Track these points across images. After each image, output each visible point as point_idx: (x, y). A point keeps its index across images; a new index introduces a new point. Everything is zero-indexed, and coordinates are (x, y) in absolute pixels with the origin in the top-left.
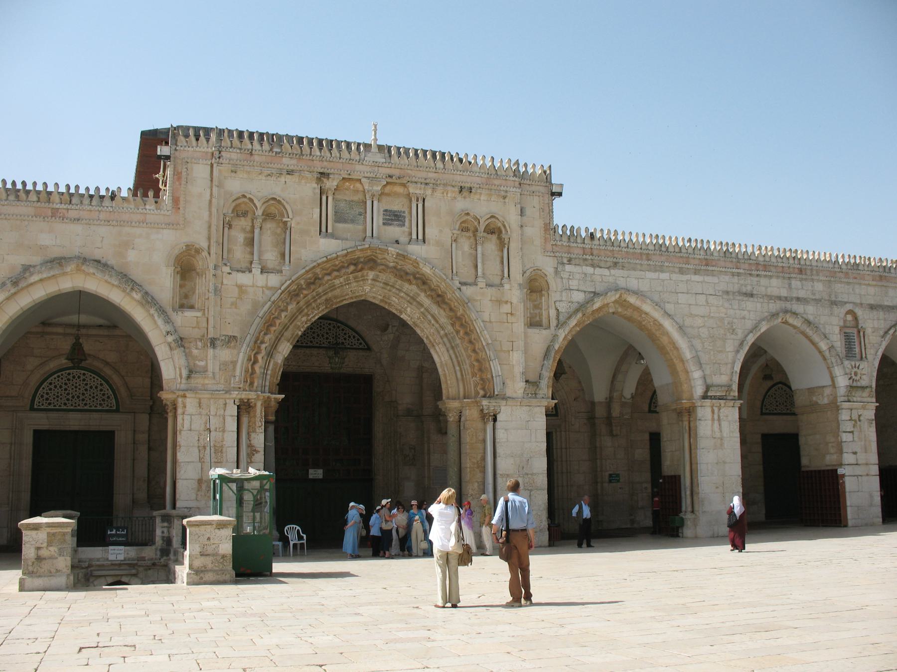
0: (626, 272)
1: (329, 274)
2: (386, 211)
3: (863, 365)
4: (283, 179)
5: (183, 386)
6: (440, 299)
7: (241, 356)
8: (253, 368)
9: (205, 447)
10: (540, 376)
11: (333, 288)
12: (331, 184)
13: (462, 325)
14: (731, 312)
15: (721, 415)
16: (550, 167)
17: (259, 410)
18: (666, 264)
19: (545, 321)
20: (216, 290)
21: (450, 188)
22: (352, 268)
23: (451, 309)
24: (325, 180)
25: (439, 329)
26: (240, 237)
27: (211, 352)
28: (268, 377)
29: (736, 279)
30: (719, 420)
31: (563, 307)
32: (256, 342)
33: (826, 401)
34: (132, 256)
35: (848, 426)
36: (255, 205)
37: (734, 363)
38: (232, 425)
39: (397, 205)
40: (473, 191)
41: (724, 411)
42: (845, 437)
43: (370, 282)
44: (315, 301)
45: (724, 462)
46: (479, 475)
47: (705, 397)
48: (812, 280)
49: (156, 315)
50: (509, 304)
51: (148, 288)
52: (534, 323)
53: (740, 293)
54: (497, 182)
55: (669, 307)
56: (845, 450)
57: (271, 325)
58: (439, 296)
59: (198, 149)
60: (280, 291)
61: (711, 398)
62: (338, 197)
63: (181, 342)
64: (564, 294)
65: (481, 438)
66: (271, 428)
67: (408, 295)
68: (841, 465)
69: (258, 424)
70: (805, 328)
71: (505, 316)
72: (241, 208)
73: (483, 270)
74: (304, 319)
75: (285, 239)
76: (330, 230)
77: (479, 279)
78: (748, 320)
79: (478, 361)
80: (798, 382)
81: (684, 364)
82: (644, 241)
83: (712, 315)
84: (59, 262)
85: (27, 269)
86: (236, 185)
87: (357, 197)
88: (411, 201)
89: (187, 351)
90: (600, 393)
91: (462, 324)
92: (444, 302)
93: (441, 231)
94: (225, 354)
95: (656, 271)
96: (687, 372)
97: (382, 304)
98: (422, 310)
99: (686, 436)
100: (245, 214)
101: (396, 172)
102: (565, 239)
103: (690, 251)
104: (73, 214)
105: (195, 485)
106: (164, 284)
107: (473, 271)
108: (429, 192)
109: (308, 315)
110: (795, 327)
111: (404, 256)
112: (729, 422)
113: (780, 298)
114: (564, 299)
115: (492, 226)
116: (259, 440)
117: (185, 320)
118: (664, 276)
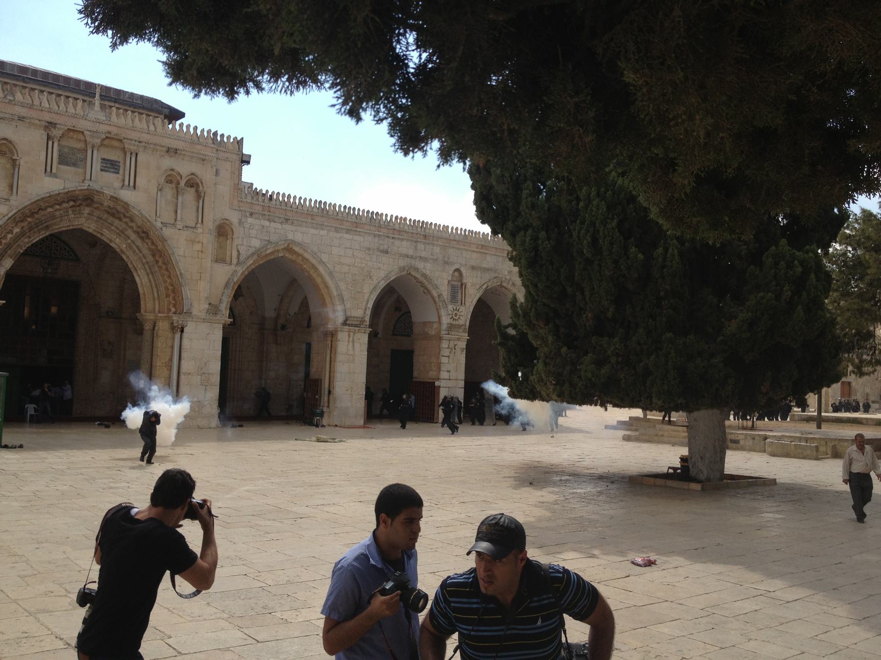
3: (462, 308)
6: (144, 234)
10: (221, 301)
11: (53, 217)
19: (228, 259)
21: (158, 147)
22: (72, 203)
23: (153, 243)
24: (52, 129)
33: (433, 333)
35: (445, 352)
37: (368, 301)
39: (114, 155)
41: (358, 335)
42: (444, 360)
45: (354, 373)
47: (345, 323)
48: (433, 244)
52: (220, 260)
53: (379, 250)
54: (199, 147)
55: (325, 258)
56: (442, 369)
58: (144, 232)
60: (7, 218)
61: (349, 325)
62: (62, 143)
64: (245, 240)
68: (438, 379)
70: (422, 279)
74: (26, 240)
76: (54, 171)
77: (178, 223)
78: (383, 271)
79: (172, 285)
80: (417, 318)
87: (80, 145)
88: (125, 153)
90: (270, 313)
92: (148, 237)
99: (329, 352)
101: (114, 130)
102: (249, 197)
108: (141, 149)
110: (416, 278)
111: (116, 198)
113: (407, 256)
115: (192, 182)
118: (323, 233)
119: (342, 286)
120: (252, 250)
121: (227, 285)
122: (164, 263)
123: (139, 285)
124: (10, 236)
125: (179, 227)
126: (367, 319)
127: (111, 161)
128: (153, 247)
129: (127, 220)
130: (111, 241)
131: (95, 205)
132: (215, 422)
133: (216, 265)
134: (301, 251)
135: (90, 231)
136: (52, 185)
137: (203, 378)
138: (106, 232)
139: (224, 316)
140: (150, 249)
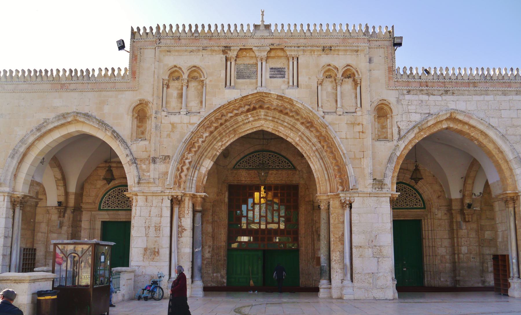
0: (455, 97)
1: (231, 112)
2: (272, 69)
4: (201, 53)
6: (310, 124)
7: (171, 168)
8: (180, 176)
10: (385, 176)
12: (232, 54)
16: (393, 27)
17: (188, 204)
18: (491, 89)
19: (389, 136)
20: (156, 127)
21: (315, 48)
23: (317, 131)
24: (229, 52)
25: (312, 146)
26: (173, 92)
27: (152, 166)
28: (194, 182)
31: (404, 127)
32: (182, 159)
34: (106, 109)
36: (182, 71)
38: (167, 213)
39: (278, 64)
40: (332, 48)
43: (263, 117)
44: (225, 131)
46: (340, 246)
49: (120, 145)
50: (361, 126)
52: (382, 136)
54: (350, 41)
55: (494, 122)
57: (192, 147)
58: (309, 122)
60: (196, 125)
62: (239, 61)
63: (134, 161)
64: (404, 116)
65: (342, 220)
66: (198, 215)
67: (289, 124)
69: (186, 212)
71: (358, 134)
72: (175, 74)
73: (342, 103)
74: (220, 144)
75: (202, 93)
76: (232, 84)
79: (338, 166)
81: (508, 163)
82: (471, 74)
84: (64, 116)
85: (46, 122)
86: (171, 61)
87: (252, 61)
88: (288, 59)
89: (139, 166)
91: (326, 141)
92: (312, 126)
93: (310, 78)
94: (161, 167)
95: (482, 94)
96: (511, 169)
97: (273, 132)
98: (300, 133)
100: (178, 78)
101: (276, 42)
104: (72, 87)
105: (142, 251)
106: (126, 125)
107: (335, 104)
108: (301, 53)
109: (223, 141)
114: (404, 119)
115: (349, 73)
116: (187, 222)
117: (139, 148)
118: (487, 98)
120: (413, 124)
121: (390, 160)
122: (328, 147)
123: (314, 171)
124: (201, 140)
125: (339, 113)
127: (279, 68)
128: (318, 134)
129: (294, 114)
130: (287, 137)
131: (266, 106)
132: (391, 292)
133: (378, 143)
134: (466, 119)
135: (270, 130)
136: (232, 95)
137: (375, 250)
138: (281, 129)
139: (391, 189)
140: (318, 137)
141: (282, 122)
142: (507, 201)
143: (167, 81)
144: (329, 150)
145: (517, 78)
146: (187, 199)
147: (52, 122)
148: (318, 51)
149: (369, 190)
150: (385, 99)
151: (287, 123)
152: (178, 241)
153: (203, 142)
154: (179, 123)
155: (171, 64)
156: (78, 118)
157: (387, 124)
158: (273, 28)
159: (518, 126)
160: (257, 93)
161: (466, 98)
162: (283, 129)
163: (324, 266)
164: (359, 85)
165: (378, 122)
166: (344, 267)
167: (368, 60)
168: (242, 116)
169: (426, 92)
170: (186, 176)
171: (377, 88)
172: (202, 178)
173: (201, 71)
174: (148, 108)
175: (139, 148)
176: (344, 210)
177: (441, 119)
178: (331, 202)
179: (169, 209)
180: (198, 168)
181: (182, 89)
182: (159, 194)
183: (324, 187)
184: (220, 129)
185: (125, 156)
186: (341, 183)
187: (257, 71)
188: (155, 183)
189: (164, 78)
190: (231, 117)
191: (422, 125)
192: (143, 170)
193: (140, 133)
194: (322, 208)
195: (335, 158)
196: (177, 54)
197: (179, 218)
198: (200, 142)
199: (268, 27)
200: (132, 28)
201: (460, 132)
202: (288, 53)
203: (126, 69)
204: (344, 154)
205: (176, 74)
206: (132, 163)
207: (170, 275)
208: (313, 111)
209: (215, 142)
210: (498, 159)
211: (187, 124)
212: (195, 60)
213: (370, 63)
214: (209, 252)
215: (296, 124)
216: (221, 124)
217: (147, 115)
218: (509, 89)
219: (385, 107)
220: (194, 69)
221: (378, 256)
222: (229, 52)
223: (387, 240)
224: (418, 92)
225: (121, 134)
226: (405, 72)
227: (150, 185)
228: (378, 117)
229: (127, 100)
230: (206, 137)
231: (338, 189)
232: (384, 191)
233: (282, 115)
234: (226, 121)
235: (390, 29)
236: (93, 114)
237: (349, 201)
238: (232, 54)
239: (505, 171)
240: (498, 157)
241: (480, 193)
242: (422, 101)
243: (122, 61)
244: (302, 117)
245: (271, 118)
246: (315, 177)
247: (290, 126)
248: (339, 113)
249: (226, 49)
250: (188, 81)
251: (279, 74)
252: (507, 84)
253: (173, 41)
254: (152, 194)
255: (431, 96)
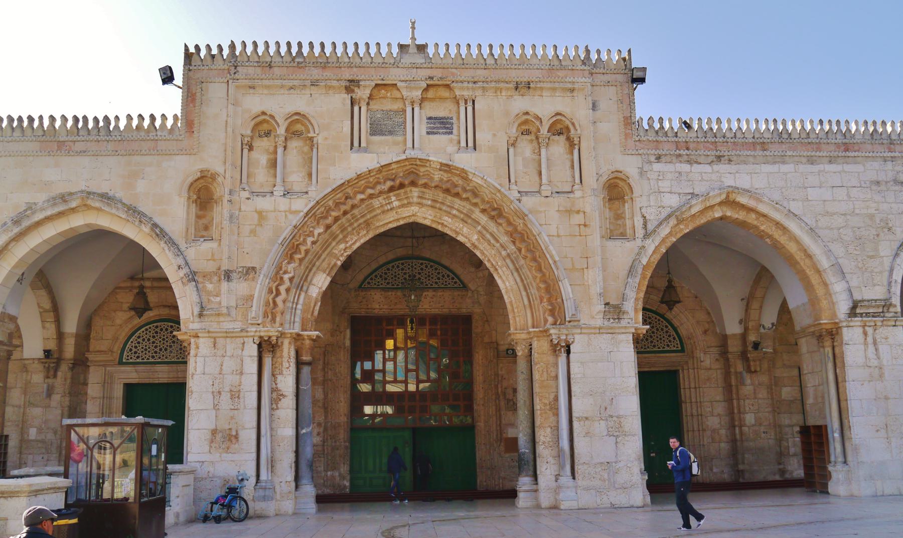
0: (734, 167)
1: (362, 192)
2: (430, 118)
4: (308, 92)
5: (195, 326)
6: (496, 212)
7: (259, 288)
9: (219, 393)
10: (624, 298)
12: (362, 93)
13: (523, 240)
14: (885, 207)
15: (878, 337)
16: (629, 51)
17: (288, 351)
18: (789, 153)
20: (231, 217)
21: (502, 85)
23: (509, 223)
24: (356, 89)
25: (500, 248)
26: (261, 157)
27: (225, 285)
28: (298, 312)
29: (889, 165)
30: (875, 343)
32: (277, 273)
34: (141, 186)
39: (441, 110)
40: (532, 85)
43: (415, 200)
44: (351, 224)
45: (886, 398)
46: (552, 419)
47: (853, 313)
49: (166, 248)
50: (582, 215)
51: (157, 220)
52: (616, 231)
54: (561, 74)
55: (795, 207)
57: (295, 253)
58: (494, 209)
59: (213, 67)
60: (302, 214)
62: (374, 106)
63: (192, 277)
64: (652, 198)
65: (553, 374)
67: (461, 212)
69: (285, 365)
71: (577, 228)
72: (262, 126)
73: (549, 176)
74: (342, 246)
75: (311, 158)
76: (363, 144)
79: (545, 282)
81: (820, 275)
82: (757, 129)
83: (857, 211)
84: (63, 198)
85: (31, 207)
86: (255, 103)
87: (397, 106)
88: (458, 103)
89: (200, 286)
91: (523, 239)
92: (500, 215)
93: (494, 135)
94: (240, 287)
95: (775, 163)
96: (826, 285)
97: (434, 226)
98: (479, 228)
99: (830, 365)
100: (268, 134)
101: (437, 73)
103: (822, 135)
104: (79, 146)
105: (209, 436)
106: (176, 215)
107: (537, 178)
108: (479, 93)
109: (347, 242)
112: (891, 345)
114: (652, 204)
115: (559, 126)
116: (287, 382)
117: (200, 254)
118: (785, 168)
119: (838, 249)
120: (667, 211)
121: (631, 272)
122: (528, 250)
123: (503, 292)
124: (310, 240)
125: (544, 193)
126: (896, 300)
127: (442, 118)
128: (510, 229)
129: (469, 195)
130: (457, 233)
131: (422, 182)
132: (639, 495)
133: (611, 244)
134: (752, 203)
135: (427, 222)
137: (611, 424)
138: (447, 220)
139: (634, 320)
141: (448, 209)
142: (821, 336)
143: (249, 139)
144: (529, 255)
145: (830, 135)
146: (286, 342)
147: (42, 209)
148: (508, 89)
149: (599, 322)
150: (621, 169)
151: (458, 210)
152: (271, 415)
153: (314, 243)
154: (271, 211)
155: (257, 109)
156: (89, 202)
157: (624, 212)
158: (431, 51)
159: (834, 214)
160: (407, 159)
161: (750, 167)
162: (450, 220)
163: (524, 454)
164: (577, 147)
165: (610, 209)
166: (559, 455)
167: (591, 106)
168: (380, 198)
169: (686, 158)
170: (284, 302)
171: (606, 155)
172: (312, 305)
173: (310, 121)
174: (215, 185)
175: (200, 254)
176: (557, 356)
177: (713, 202)
178: (535, 345)
179: (256, 359)
180: (305, 288)
181: (275, 152)
182: (237, 335)
183: (521, 317)
184: (344, 220)
185: (176, 268)
186: (551, 311)
187: (405, 122)
188: (229, 315)
189: (244, 133)
190: (362, 200)
191: (682, 213)
192: (209, 293)
193: (203, 228)
194: (519, 354)
195: (540, 269)
196: (266, 91)
197: (273, 375)
198: (309, 243)
199: (422, 48)
200: (186, 46)
201: (743, 224)
202: (458, 93)
203: (175, 117)
204: (555, 262)
205: (265, 127)
206: (189, 281)
207: (258, 476)
208: (502, 190)
209: (334, 244)
210: (805, 268)
211: (285, 212)
212: (298, 103)
213: (593, 110)
214: (318, 434)
215: (473, 211)
216: (345, 213)
217: (215, 197)
218: (818, 154)
219: (621, 184)
220: (296, 117)
221: (617, 433)
222: (356, 89)
223: (630, 405)
224: (674, 158)
225: (167, 229)
226: (651, 126)
227: (222, 319)
228: (610, 200)
229: (180, 170)
230: (319, 234)
231: (546, 321)
232: (624, 323)
233: (450, 198)
234: (353, 207)
235: (625, 54)
236: (117, 195)
237: (566, 341)
238: (362, 93)
239: (816, 287)
240: (804, 264)
241: (773, 324)
242: (680, 173)
243: (168, 103)
244: (483, 201)
245: (429, 203)
246: (507, 301)
247: (462, 216)
248: (544, 193)
249: (351, 85)
250: (286, 139)
251: (442, 128)
252: (815, 146)
253: (259, 70)
254: (225, 335)
255: (695, 165)
